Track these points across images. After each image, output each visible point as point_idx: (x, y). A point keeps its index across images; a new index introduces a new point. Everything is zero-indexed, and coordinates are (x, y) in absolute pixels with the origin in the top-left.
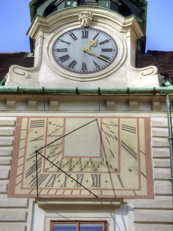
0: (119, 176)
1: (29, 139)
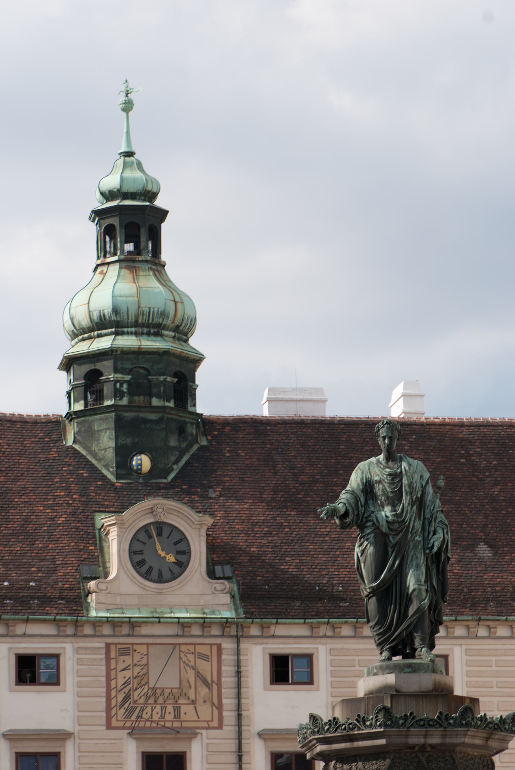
0: (195, 707)
1: (119, 669)
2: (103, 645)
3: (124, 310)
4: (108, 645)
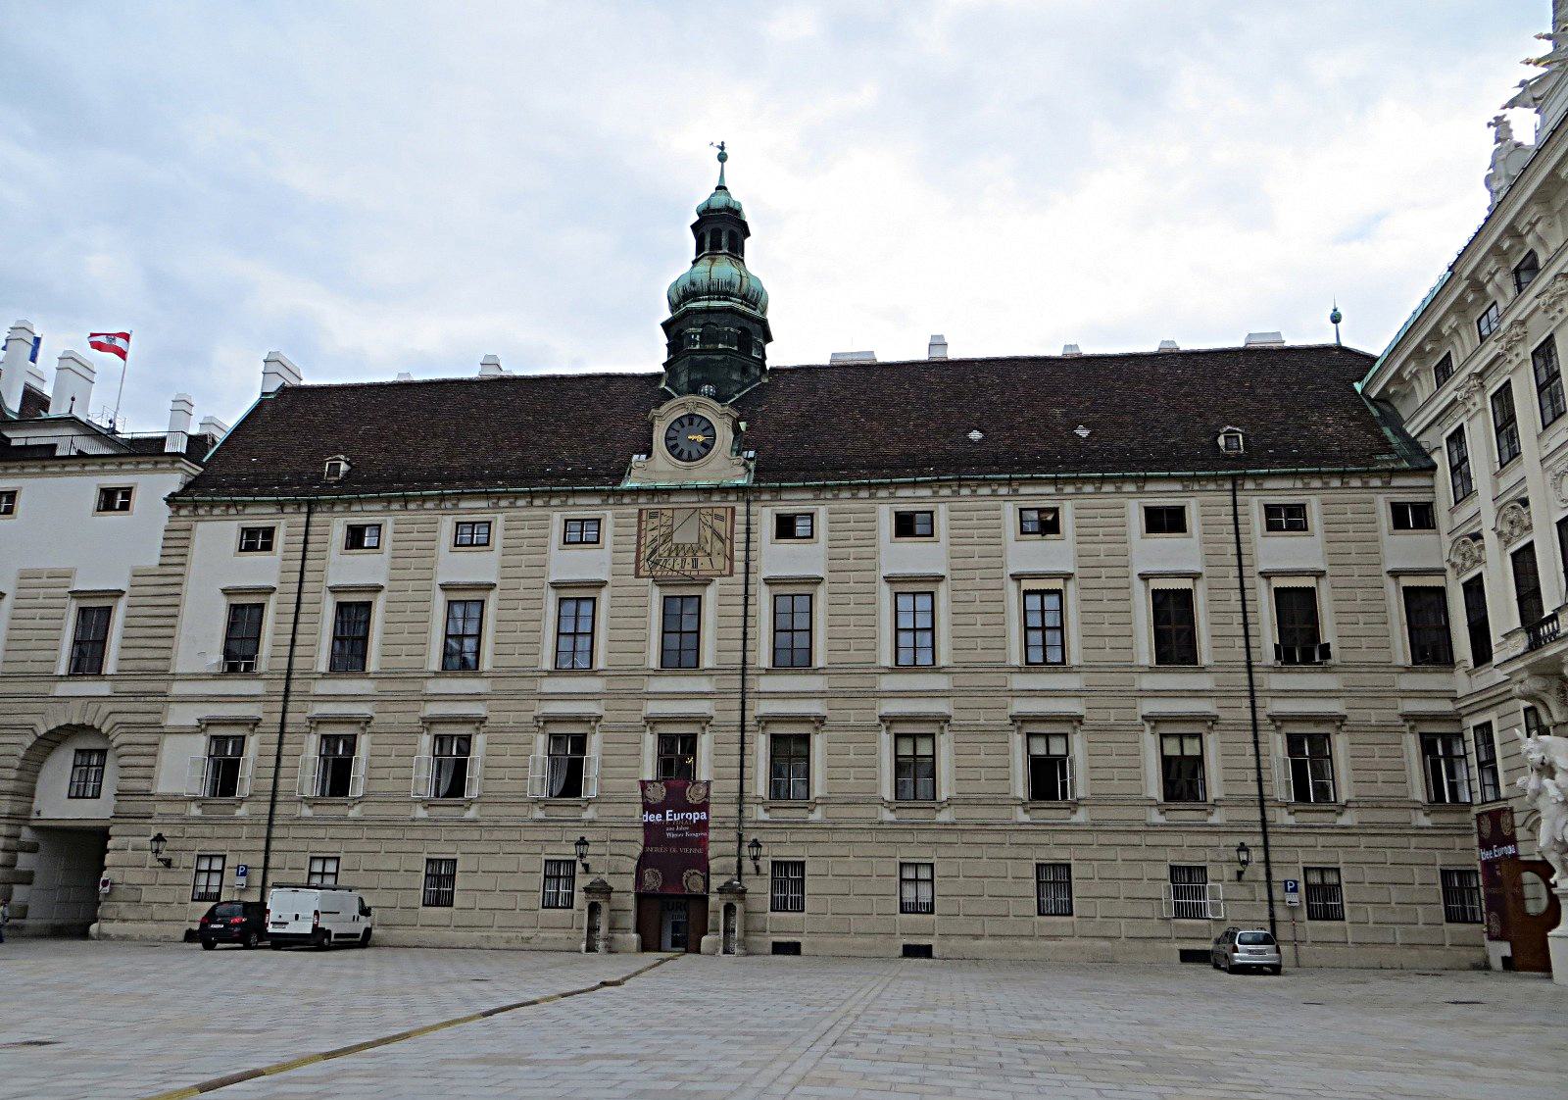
3: (698, 283)
4: (641, 511)
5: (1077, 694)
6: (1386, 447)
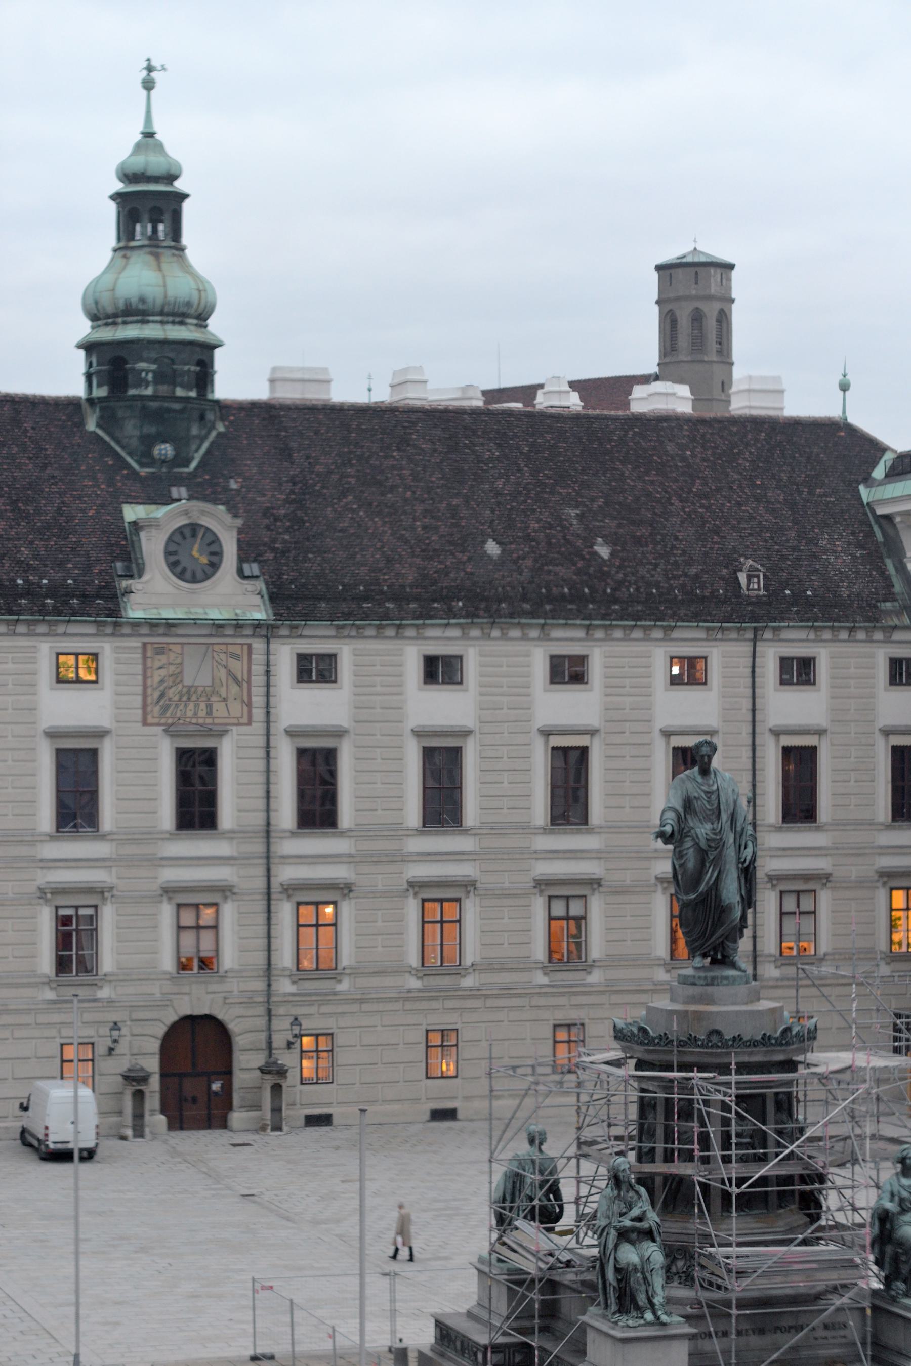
2: (139, 644)
3: (150, 300)
4: (145, 645)
5: (597, 855)
6: (890, 596)
